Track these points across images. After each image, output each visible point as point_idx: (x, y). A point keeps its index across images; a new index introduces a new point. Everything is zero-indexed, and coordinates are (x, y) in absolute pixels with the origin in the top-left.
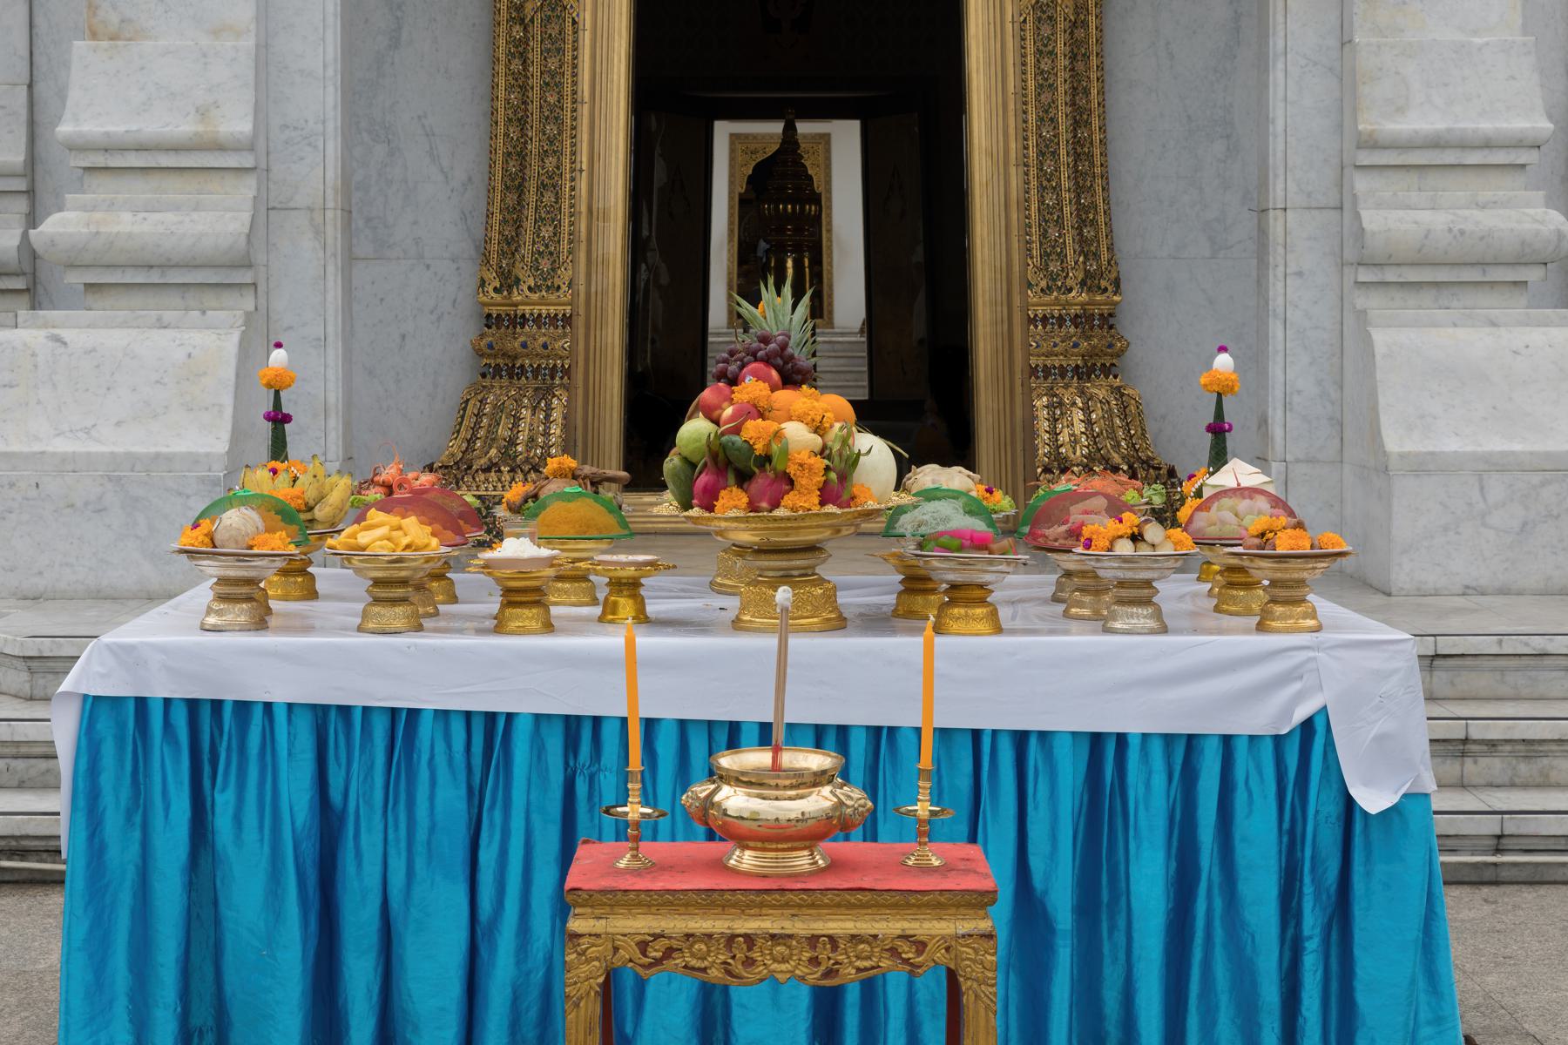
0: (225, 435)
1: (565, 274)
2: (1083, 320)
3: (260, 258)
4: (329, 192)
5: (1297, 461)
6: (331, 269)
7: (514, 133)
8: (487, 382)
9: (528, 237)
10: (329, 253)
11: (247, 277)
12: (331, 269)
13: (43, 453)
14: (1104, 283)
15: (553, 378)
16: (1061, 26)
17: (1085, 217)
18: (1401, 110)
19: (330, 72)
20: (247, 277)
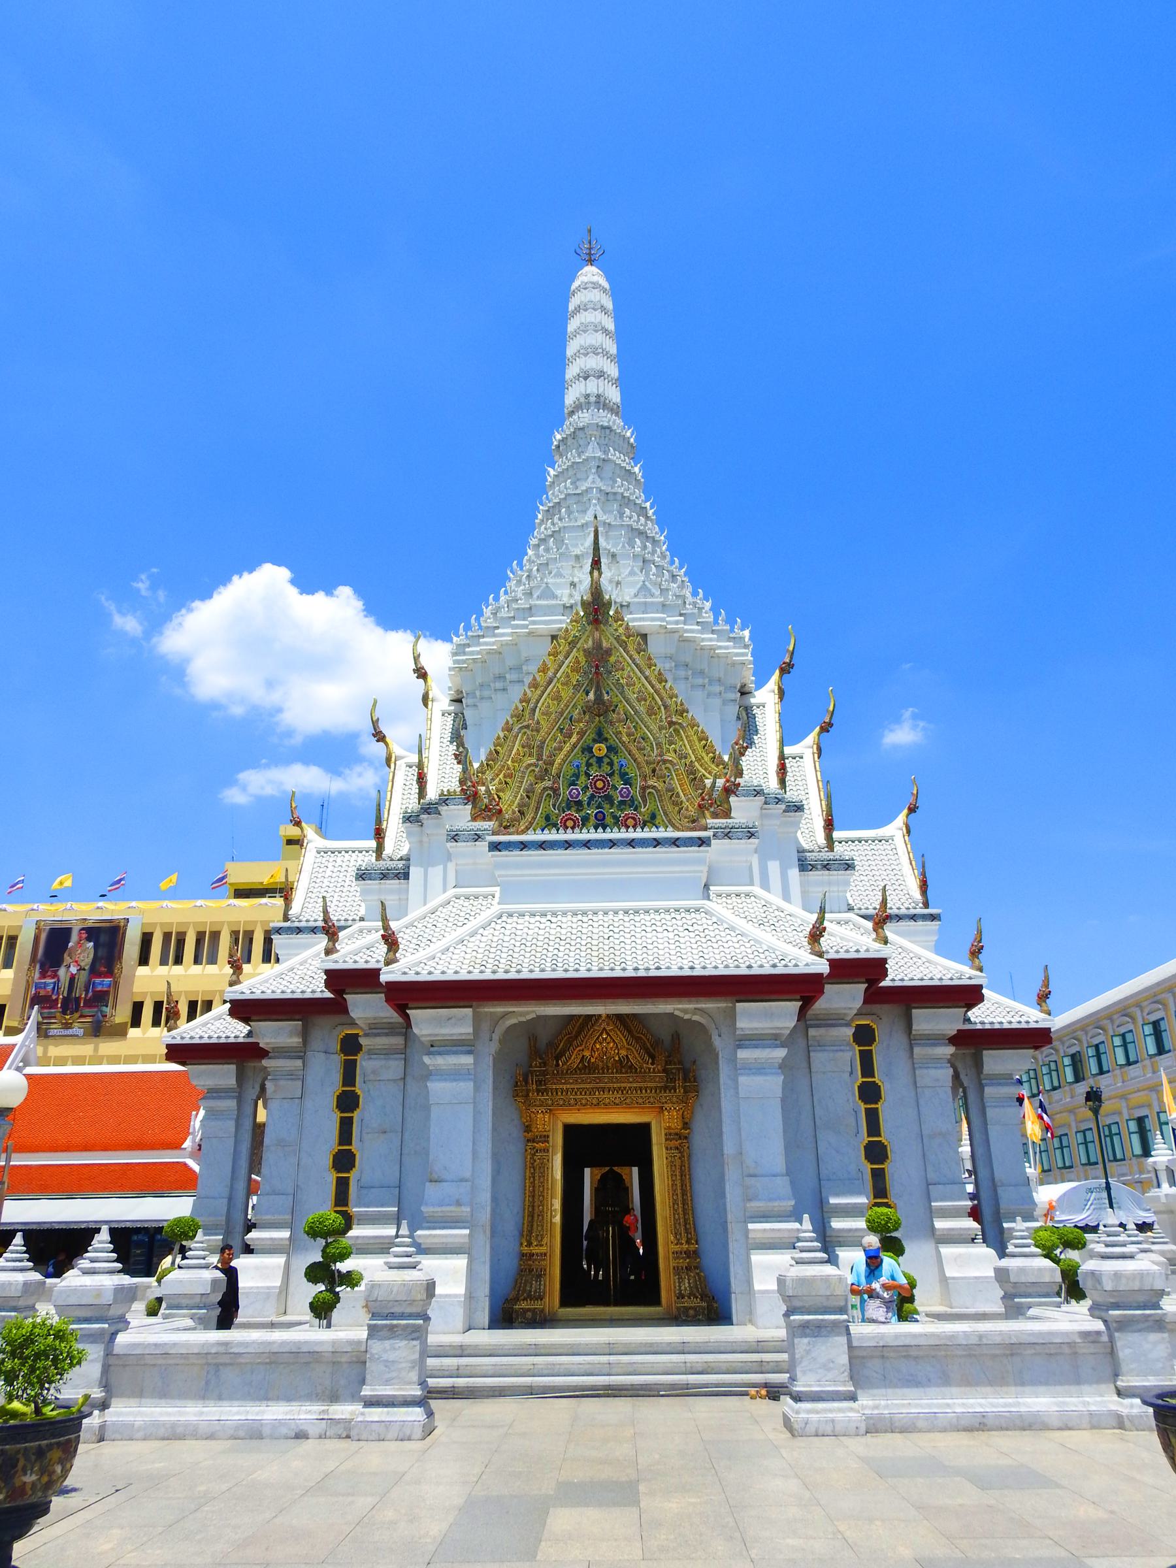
1: (544, 1242)
2: (688, 1254)
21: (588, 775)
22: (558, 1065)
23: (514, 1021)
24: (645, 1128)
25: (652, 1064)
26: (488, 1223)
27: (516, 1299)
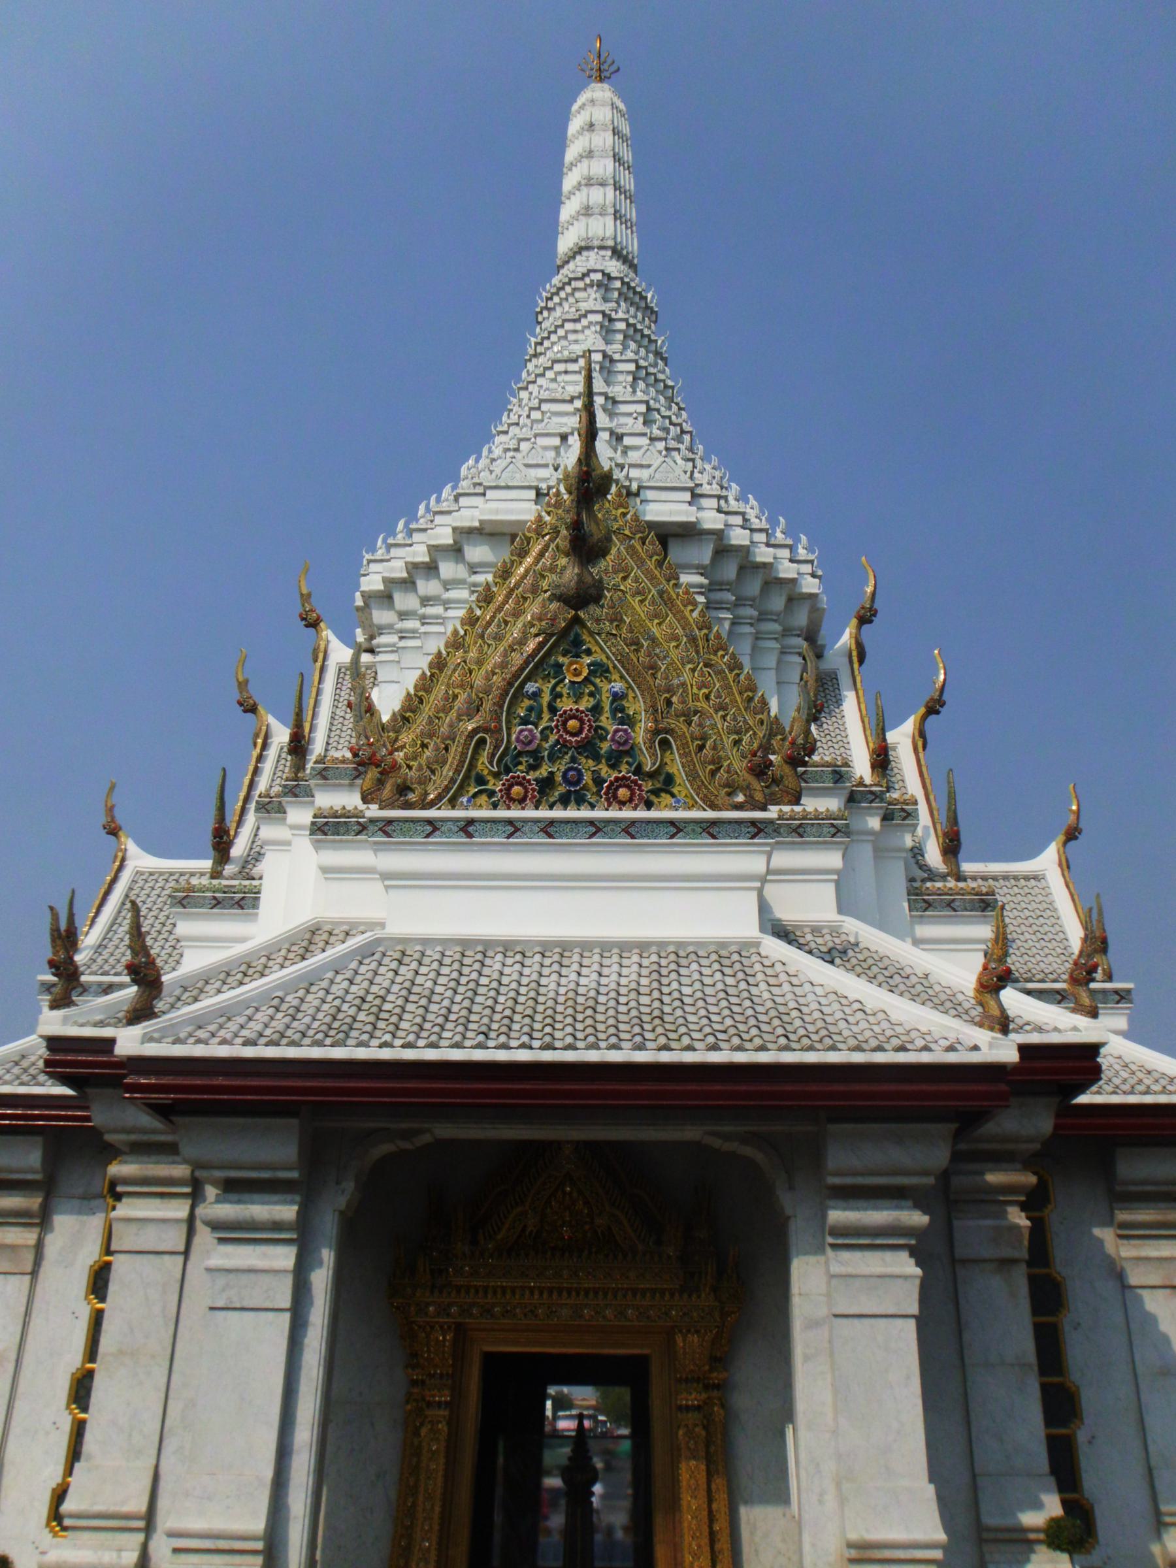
21: (553, 710)
23: (386, 1148)
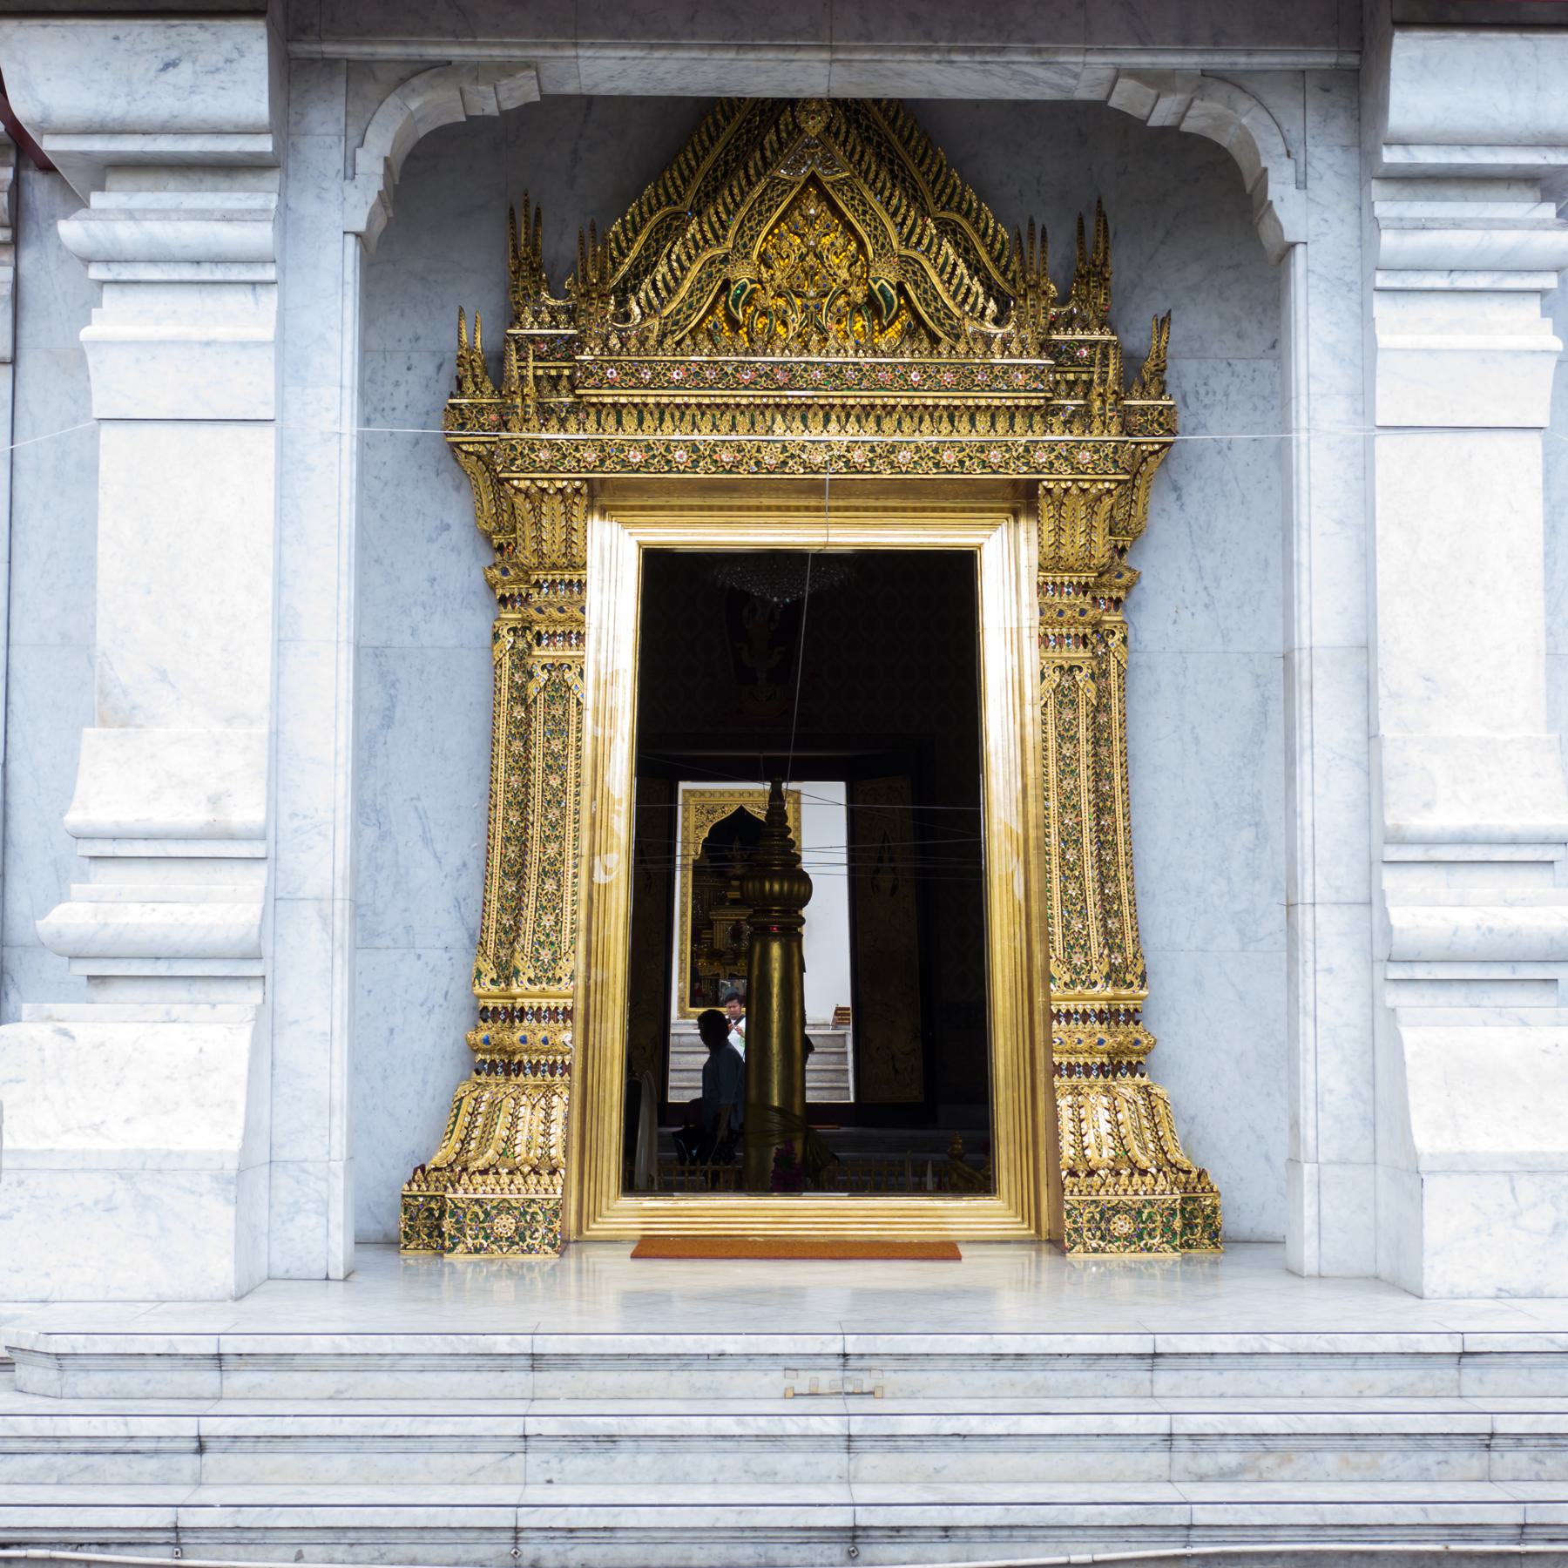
0: (238, 1131)
1: (566, 966)
3: (267, 950)
4: (338, 882)
5: (1330, 1162)
6: (338, 961)
7: (514, 817)
8: (483, 1078)
9: (528, 926)
10: (337, 945)
11: (254, 969)
12: (338, 961)
13: (52, 1150)
14: (1129, 977)
15: (553, 1075)
16: (1083, 710)
17: (1109, 906)
18: (1428, 805)
19: (341, 760)
20: (254, 969)
22: (627, 317)
24: (955, 574)
25: (997, 321)
26: (342, 892)
27: (458, 1169)
